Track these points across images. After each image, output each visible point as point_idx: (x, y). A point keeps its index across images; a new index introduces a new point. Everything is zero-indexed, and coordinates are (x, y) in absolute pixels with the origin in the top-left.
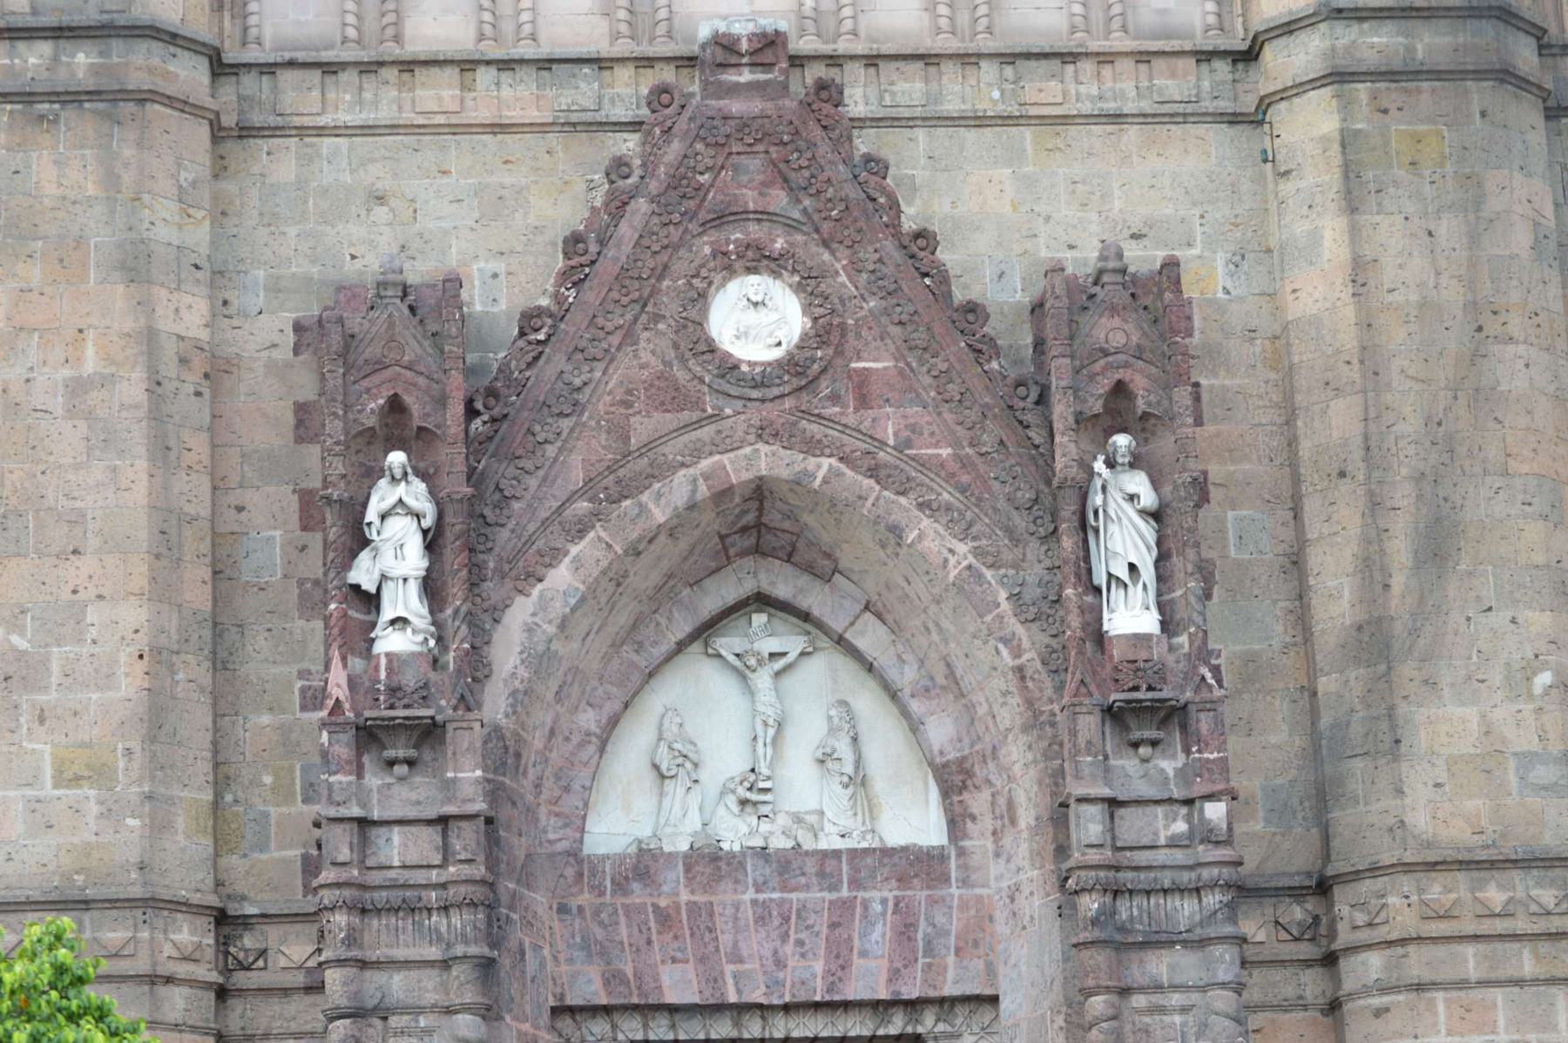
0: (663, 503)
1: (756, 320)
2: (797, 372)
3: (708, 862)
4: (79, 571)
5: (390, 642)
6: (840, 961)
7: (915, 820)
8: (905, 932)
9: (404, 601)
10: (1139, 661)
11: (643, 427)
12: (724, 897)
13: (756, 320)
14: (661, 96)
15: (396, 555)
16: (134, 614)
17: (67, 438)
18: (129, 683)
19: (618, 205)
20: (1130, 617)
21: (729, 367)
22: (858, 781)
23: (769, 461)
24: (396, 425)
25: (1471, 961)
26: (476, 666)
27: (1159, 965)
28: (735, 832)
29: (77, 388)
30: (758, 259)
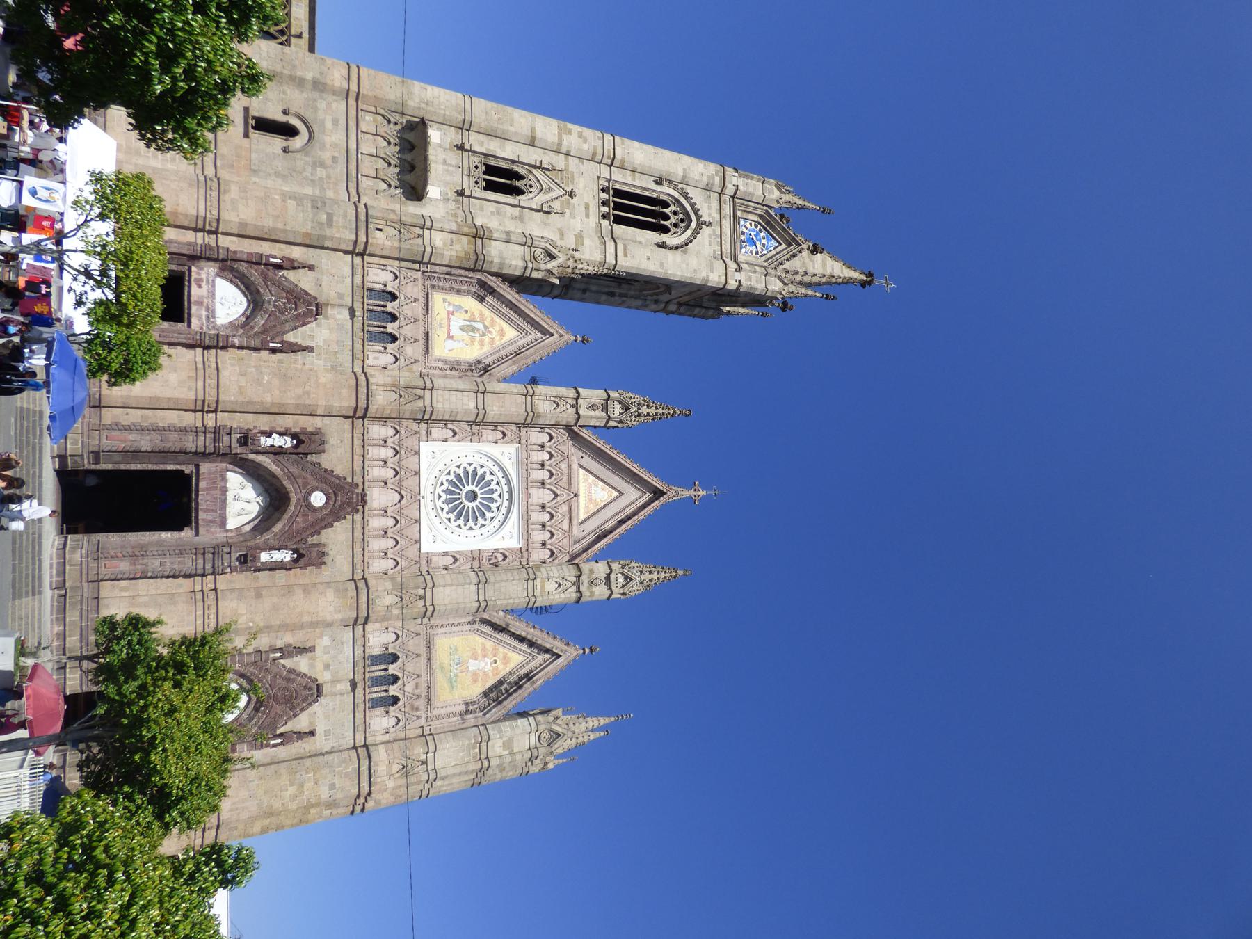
0: (286, 483)
1: (318, 499)
2: (309, 505)
3: (224, 490)
4: (277, 392)
5: (263, 439)
6: (206, 511)
7: (231, 524)
8: (211, 521)
9: (270, 442)
10: (256, 558)
11: (300, 481)
12: (218, 492)
13: (318, 499)
14: (357, 485)
15: (277, 441)
16: (269, 399)
17: (299, 391)
18: (256, 399)
19: (338, 477)
20: (264, 557)
21: (310, 494)
22: (239, 515)
23: (294, 500)
24: (300, 442)
25: (200, 612)
26: (258, 453)
27: (201, 561)
28: (230, 495)
29: (308, 393)
30: (328, 499)
